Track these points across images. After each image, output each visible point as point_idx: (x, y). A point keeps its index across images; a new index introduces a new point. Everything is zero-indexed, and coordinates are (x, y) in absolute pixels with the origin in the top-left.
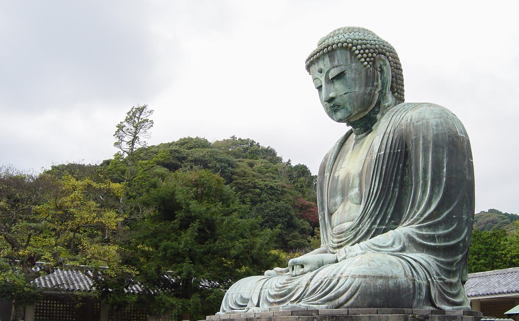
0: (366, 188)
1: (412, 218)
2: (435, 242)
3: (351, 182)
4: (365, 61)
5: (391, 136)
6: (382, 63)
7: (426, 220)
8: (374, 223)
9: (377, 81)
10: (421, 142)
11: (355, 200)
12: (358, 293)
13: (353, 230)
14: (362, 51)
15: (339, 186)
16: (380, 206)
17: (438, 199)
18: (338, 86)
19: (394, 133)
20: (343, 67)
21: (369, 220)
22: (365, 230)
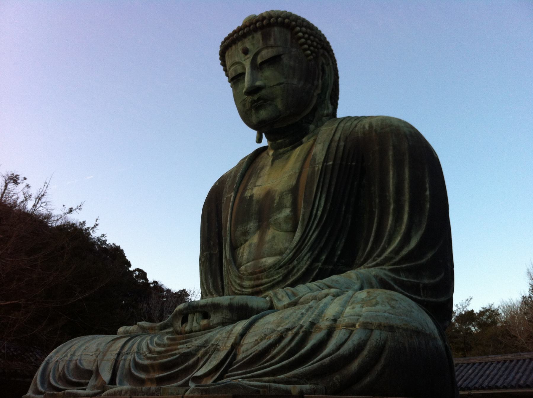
0: (305, 208)
1: (379, 256)
2: (420, 296)
3: (276, 201)
4: (309, 49)
5: (342, 144)
6: (324, 61)
7: (405, 259)
8: (316, 259)
9: (318, 80)
10: (391, 153)
11: (284, 226)
12: (382, 361)
13: (281, 267)
14: (306, 36)
15: (255, 207)
16: (327, 235)
17: (421, 232)
18: (268, 73)
19: (346, 141)
20: (281, 49)
21: (309, 254)
22: (303, 269)
